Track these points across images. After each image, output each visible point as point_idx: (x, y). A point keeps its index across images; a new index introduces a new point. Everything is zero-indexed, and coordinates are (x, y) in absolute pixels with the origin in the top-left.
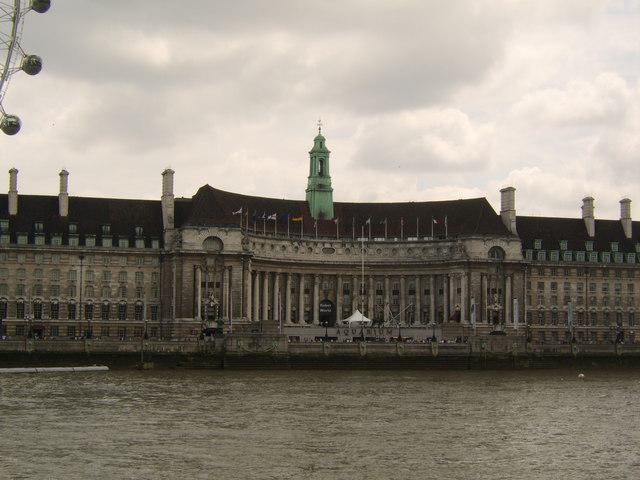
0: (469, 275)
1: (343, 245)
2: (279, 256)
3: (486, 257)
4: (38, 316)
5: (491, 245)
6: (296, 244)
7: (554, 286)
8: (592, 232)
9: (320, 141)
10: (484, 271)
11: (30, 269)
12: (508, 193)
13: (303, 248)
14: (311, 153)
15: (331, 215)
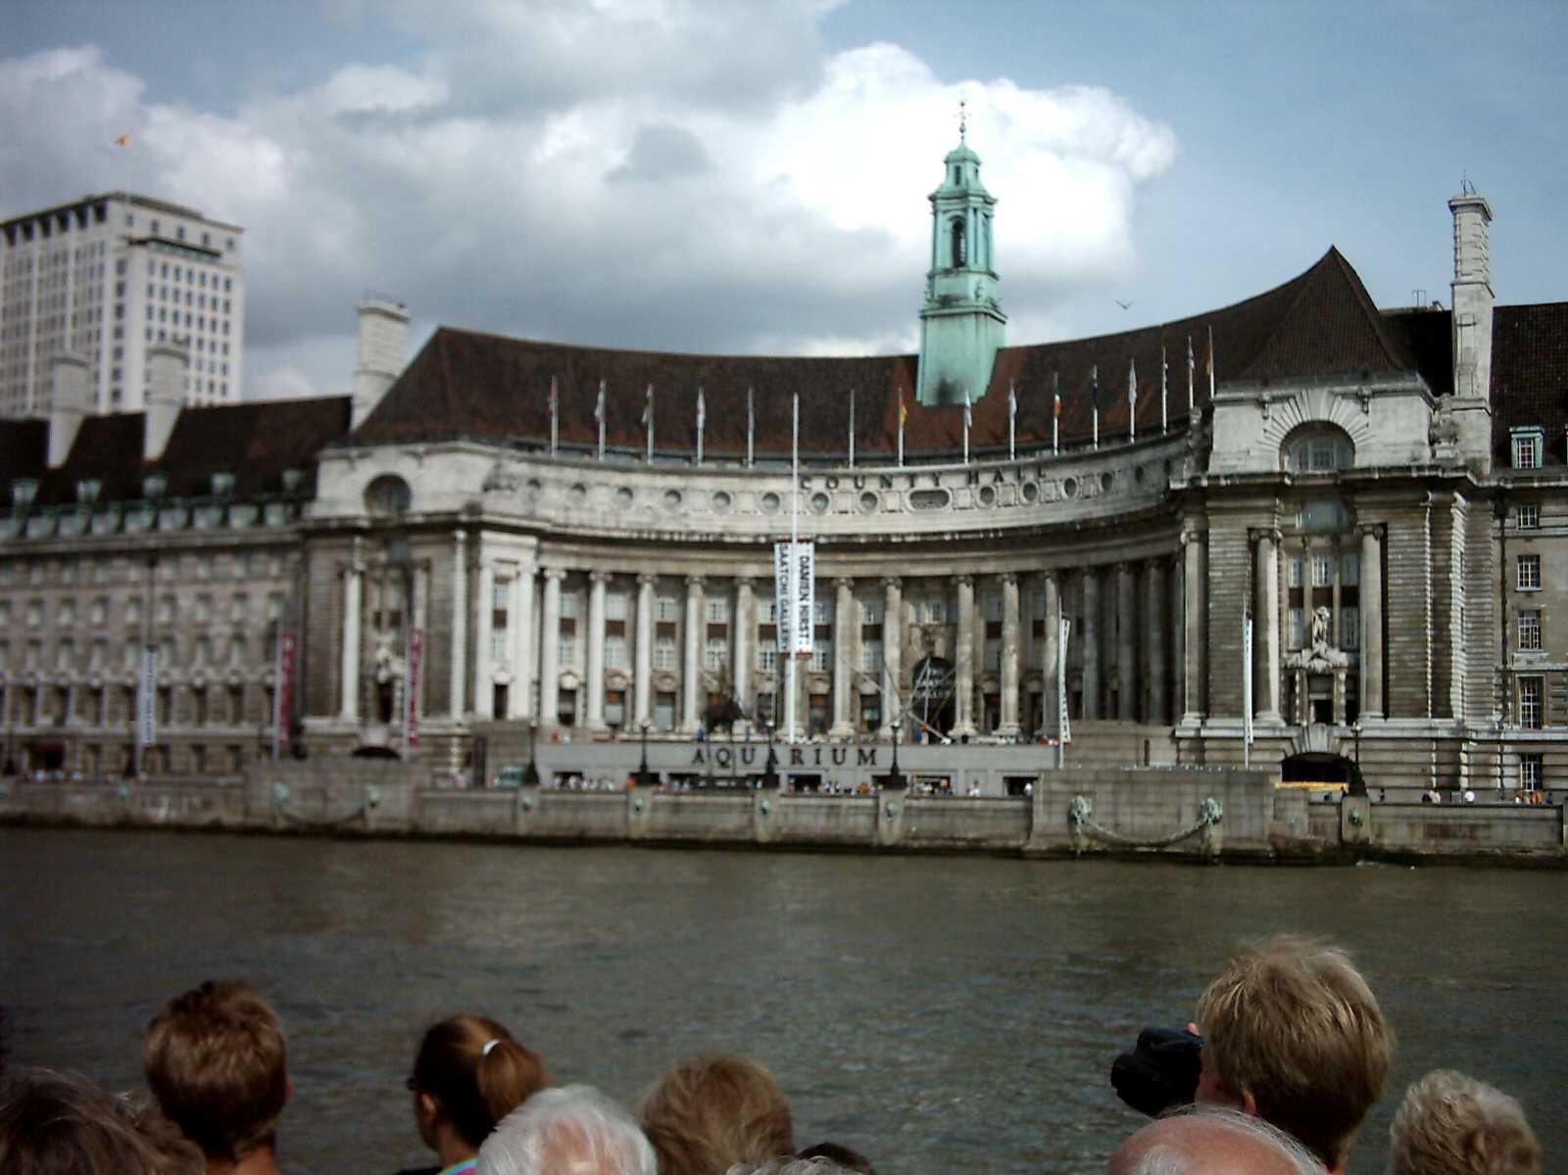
0: (1203, 538)
1: (972, 477)
4: (60, 721)
5: (1288, 417)
10: (1262, 521)
11: (50, 596)
13: (845, 495)
14: (933, 198)
15: (976, 384)
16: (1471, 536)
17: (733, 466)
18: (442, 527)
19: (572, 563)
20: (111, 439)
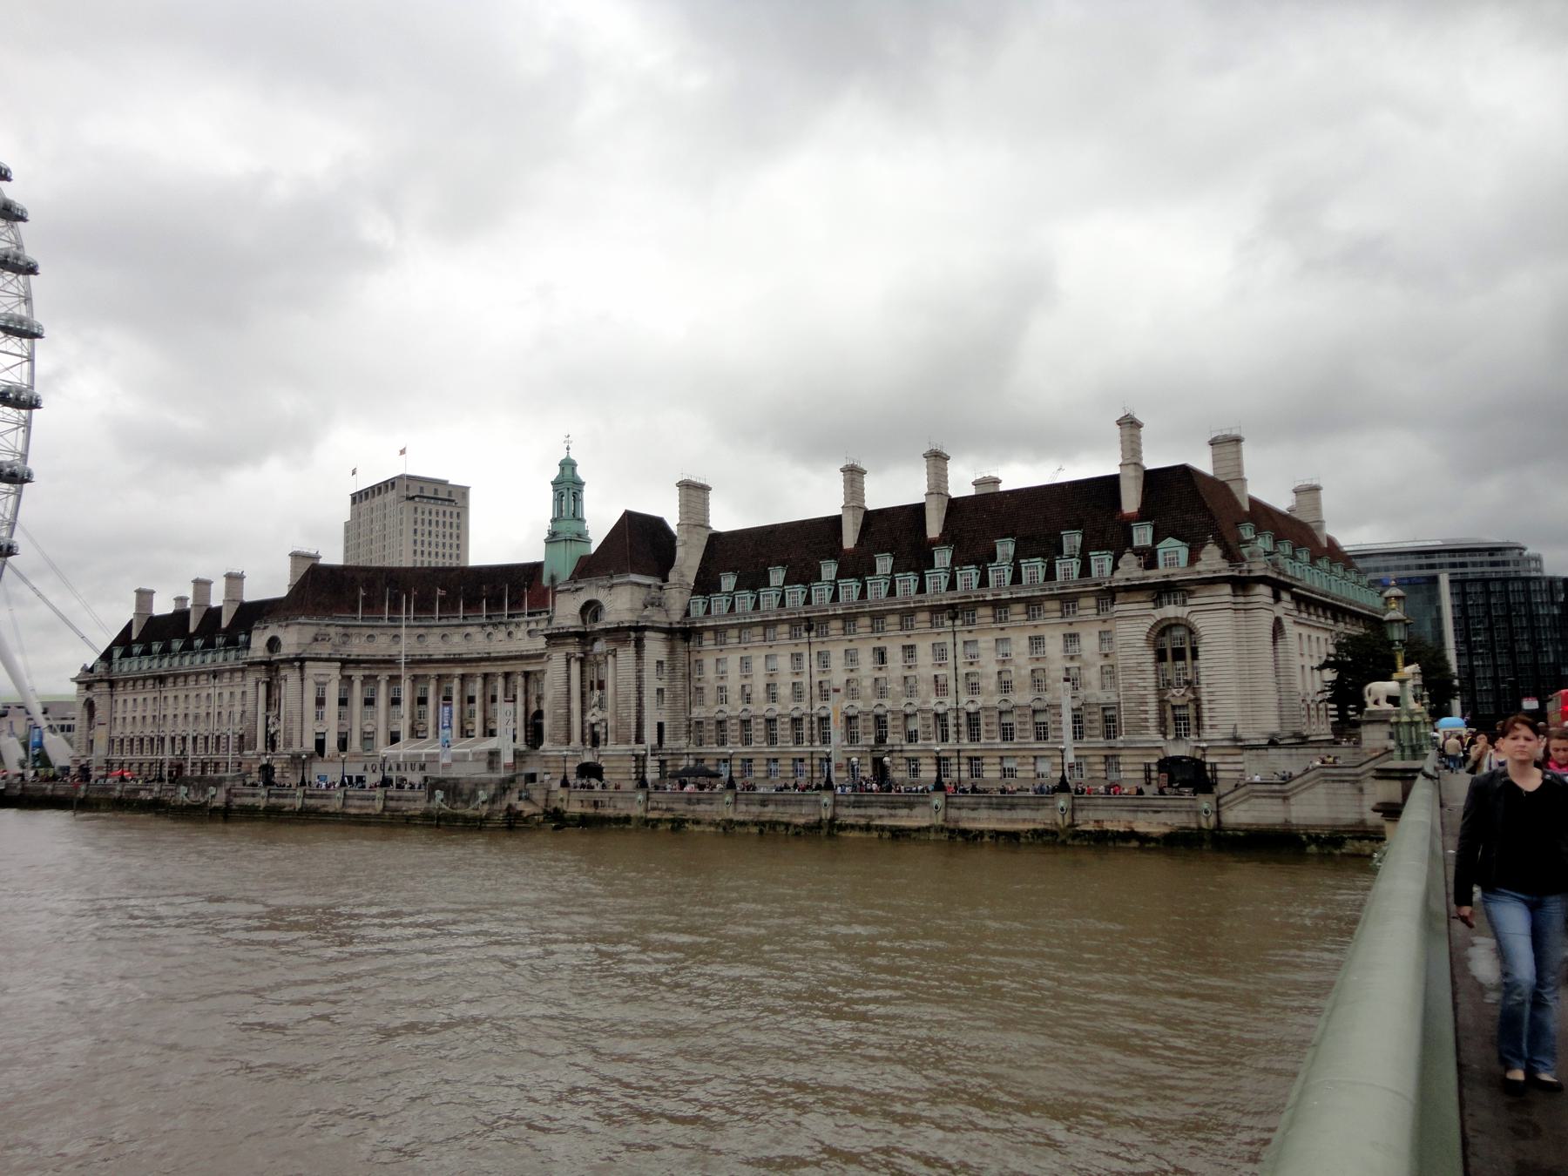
2: (457, 650)
3: (580, 623)
5: (583, 598)
6: (489, 629)
7: (745, 663)
8: (849, 540)
9: (568, 465)
10: (571, 650)
12: (694, 493)
13: (500, 634)
16: (672, 651)
17: (455, 622)
18: (289, 661)
19: (367, 672)
20: (213, 615)
